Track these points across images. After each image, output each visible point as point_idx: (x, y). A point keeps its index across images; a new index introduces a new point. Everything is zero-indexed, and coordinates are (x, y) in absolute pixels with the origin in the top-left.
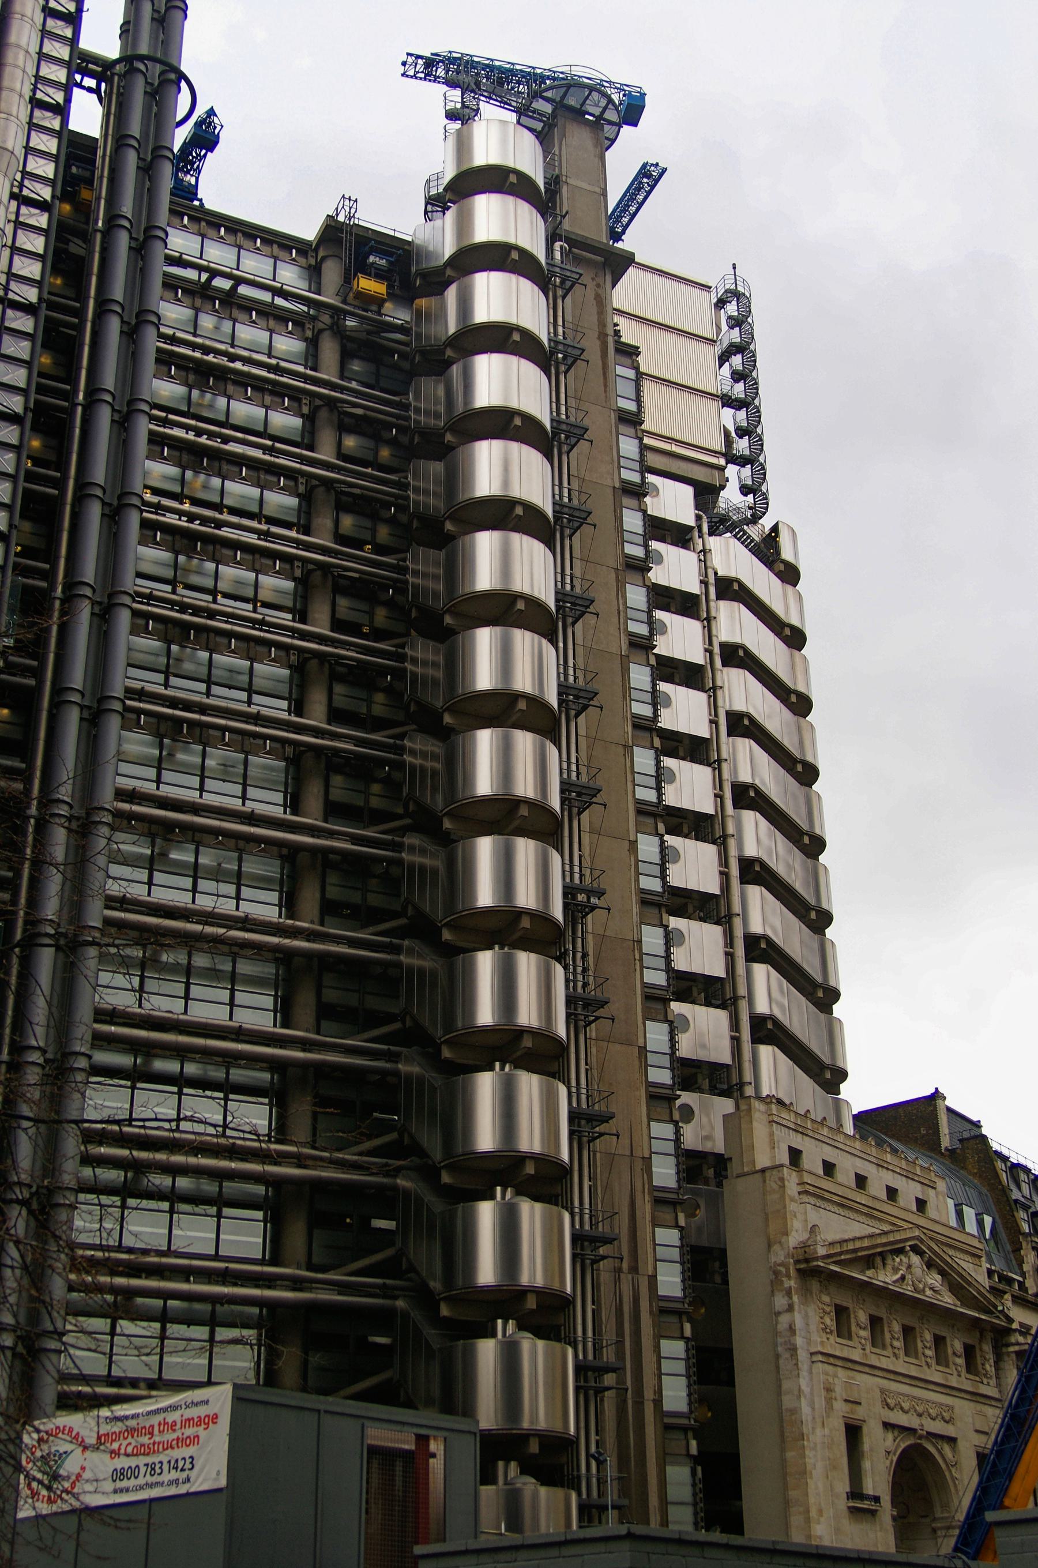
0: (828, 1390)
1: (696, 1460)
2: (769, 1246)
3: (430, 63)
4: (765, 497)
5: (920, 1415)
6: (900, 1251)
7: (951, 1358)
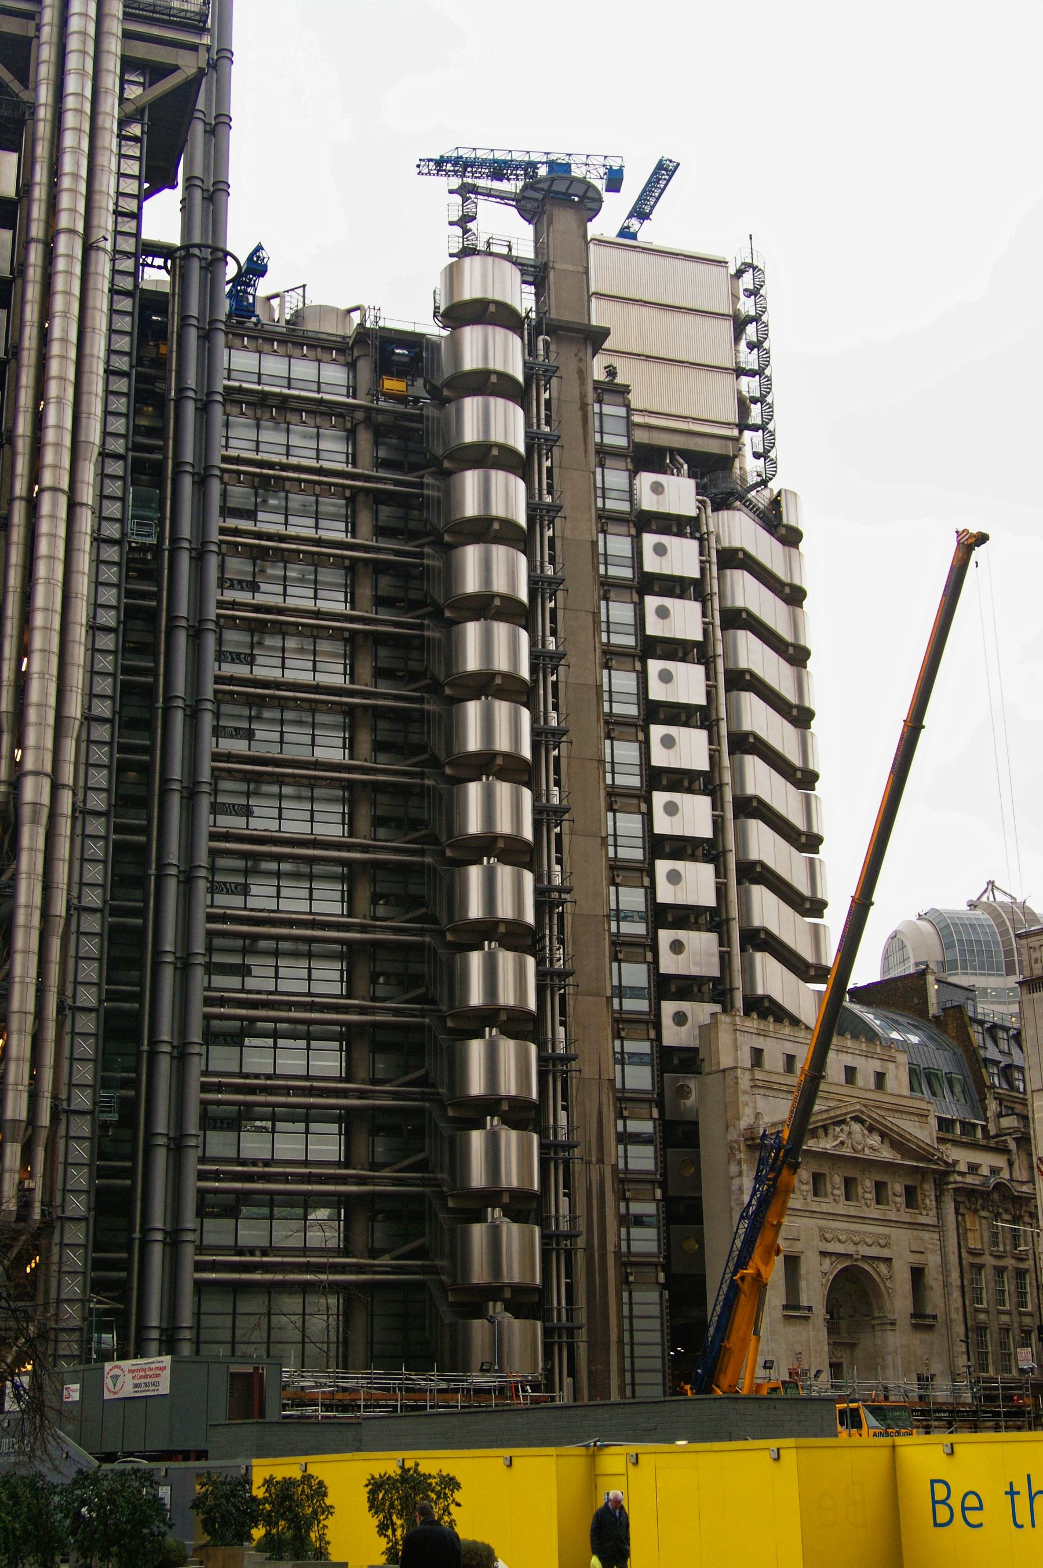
1: (664, 1286)
2: (727, 1128)
3: (440, 163)
4: (774, 462)
5: (856, 1244)
6: (843, 1122)
7: (891, 1197)
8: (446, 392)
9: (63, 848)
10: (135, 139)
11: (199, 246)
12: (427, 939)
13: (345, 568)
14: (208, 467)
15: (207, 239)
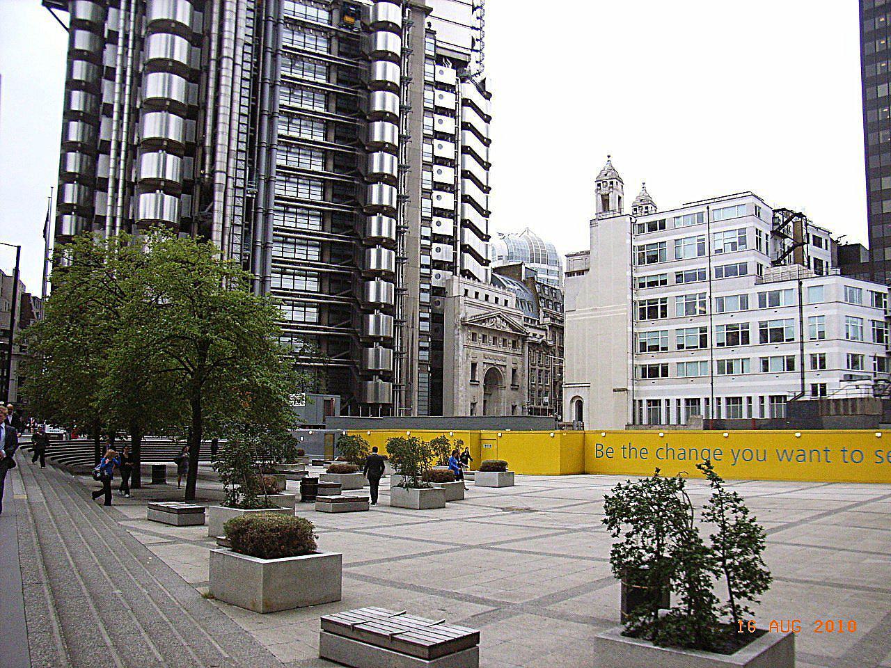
0: (467, 355)
6: (495, 317)
8: (371, 28)
12: (354, 242)
13: (325, 95)
14: (277, 50)
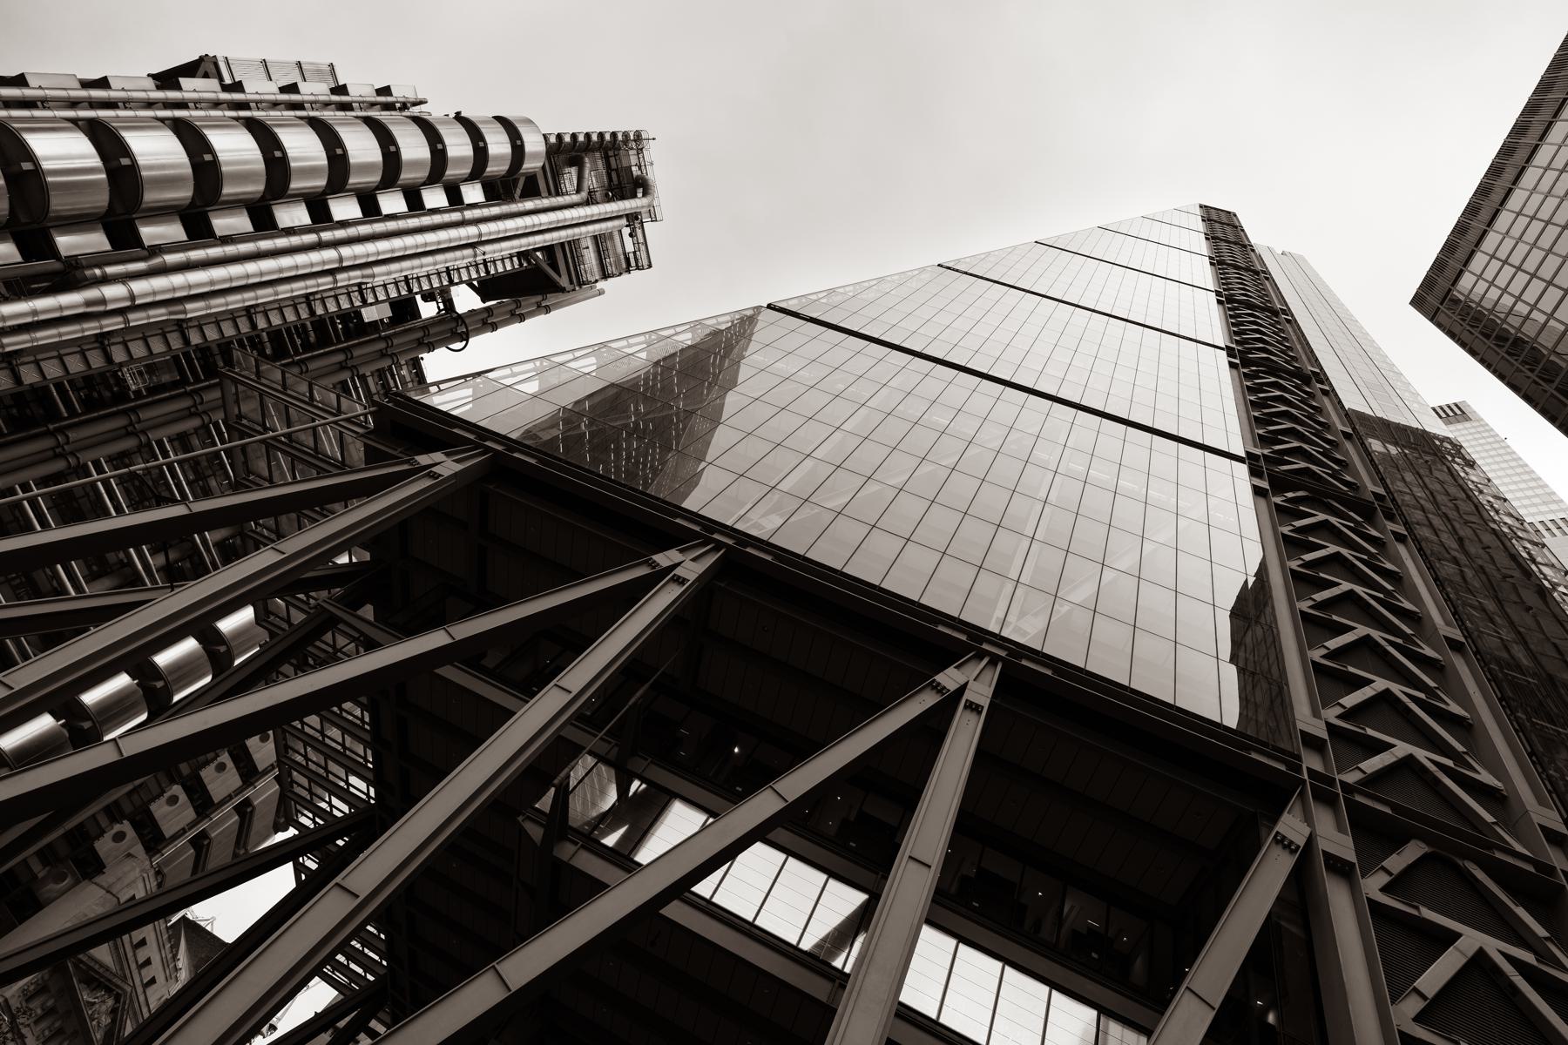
9: (70, 332)
10: (521, 265)
11: (464, 322)
15: (471, 326)
